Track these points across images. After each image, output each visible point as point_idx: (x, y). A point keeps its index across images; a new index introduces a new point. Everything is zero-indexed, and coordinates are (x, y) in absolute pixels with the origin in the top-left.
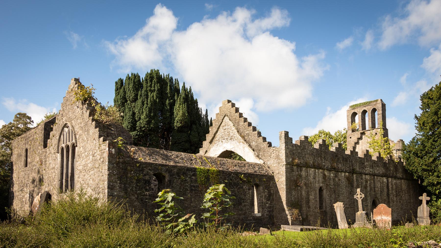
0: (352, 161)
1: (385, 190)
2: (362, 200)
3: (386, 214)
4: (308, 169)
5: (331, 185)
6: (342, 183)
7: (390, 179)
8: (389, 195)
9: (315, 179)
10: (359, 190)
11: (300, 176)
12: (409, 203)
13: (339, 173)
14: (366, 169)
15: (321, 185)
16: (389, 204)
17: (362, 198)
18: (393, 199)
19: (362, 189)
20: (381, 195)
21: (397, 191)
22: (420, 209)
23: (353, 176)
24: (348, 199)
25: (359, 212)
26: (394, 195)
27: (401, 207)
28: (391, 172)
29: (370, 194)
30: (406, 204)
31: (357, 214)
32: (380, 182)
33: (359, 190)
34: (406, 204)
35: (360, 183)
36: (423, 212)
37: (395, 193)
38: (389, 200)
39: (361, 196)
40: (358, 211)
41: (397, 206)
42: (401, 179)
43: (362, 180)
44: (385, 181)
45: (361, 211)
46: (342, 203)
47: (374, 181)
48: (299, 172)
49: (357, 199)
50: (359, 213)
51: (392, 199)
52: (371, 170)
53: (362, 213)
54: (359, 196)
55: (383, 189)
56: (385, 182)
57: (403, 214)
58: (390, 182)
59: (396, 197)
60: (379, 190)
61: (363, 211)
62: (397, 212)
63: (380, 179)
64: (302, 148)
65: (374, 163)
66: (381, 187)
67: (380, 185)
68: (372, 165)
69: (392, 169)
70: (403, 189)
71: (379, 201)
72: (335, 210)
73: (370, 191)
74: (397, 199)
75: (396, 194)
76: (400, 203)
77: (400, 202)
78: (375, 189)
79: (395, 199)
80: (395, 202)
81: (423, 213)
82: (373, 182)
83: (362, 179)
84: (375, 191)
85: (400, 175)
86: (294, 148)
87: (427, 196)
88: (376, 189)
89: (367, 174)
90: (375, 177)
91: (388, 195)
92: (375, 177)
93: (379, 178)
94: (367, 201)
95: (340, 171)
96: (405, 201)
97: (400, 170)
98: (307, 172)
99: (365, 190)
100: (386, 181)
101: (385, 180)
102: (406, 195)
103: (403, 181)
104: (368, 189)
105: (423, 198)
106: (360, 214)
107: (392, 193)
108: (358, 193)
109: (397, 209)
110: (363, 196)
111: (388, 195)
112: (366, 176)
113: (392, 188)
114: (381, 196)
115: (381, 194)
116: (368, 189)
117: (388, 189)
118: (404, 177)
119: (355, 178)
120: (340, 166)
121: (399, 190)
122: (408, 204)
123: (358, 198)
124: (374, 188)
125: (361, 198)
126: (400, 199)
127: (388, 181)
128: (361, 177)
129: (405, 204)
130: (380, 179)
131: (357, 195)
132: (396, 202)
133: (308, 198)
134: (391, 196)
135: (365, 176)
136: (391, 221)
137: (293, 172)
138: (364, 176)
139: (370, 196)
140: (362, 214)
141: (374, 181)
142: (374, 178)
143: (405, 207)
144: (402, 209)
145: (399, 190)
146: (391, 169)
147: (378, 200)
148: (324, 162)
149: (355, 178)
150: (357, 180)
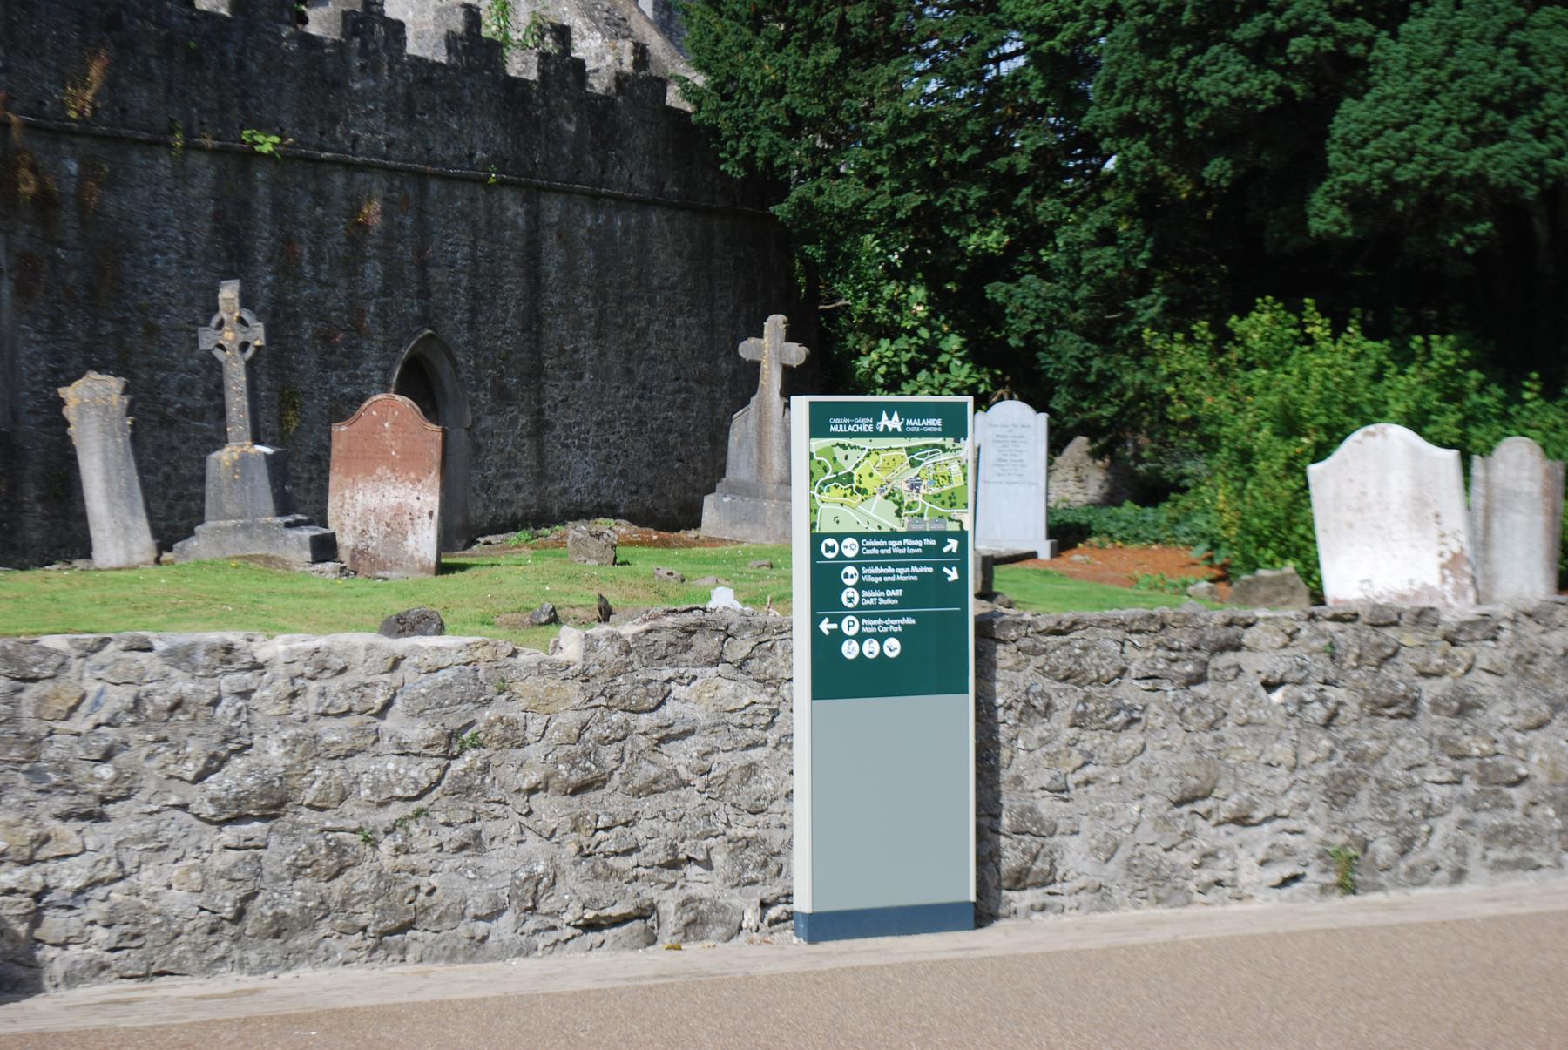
0: (241, 66)
1: (513, 285)
2: (250, 365)
3: (406, 466)
5: (61, 244)
6: (152, 226)
7: (553, 209)
8: (540, 319)
10: (229, 293)
12: (698, 381)
13: (136, 157)
16: (540, 389)
17: (250, 353)
18: (575, 351)
19: (323, 277)
22: (742, 426)
25: (227, 449)
26: (578, 325)
27: (638, 407)
28: (565, 150)
29: (383, 312)
30: (679, 391)
31: (218, 462)
32: (474, 224)
33: (229, 293)
34: (679, 391)
35: (304, 233)
36: (761, 451)
37: (587, 309)
38: (541, 360)
39: (241, 338)
40: (220, 441)
41: (600, 404)
42: (643, 204)
43: (319, 211)
44: (509, 214)
45: (239, 438)
46: (115, 384)
47: (421, 214)
49: (218, 353)
50: (224, 458)
51: (562, 351)
52: (401, 134)
53: (244, 458)
54: (228, 336)
56: (514, 226)
57: (649, 465)
58: (550, 226)
59: (599, 336)
60: (457, 283)
61: (257, 440)
62: (597, 447)
63: (473, 200)
65: (428, 81)
66: (475, 262)
67: (473, 246)
68: (408, 96)
69: (572, 128)
70: (655, 282)
71: (455, 364)
72: (72, 430)
73: (386, 291)
74: (602, 354)
75: (602, 313)
76: (631, 382)
77: (629, 371)
78: (424, 278)
79: (587, 348)
80: (588, 376)
81: (761, 464)
82: (408, 222)
83: (320, 198)
84: (425, 293)
85: (633, 174)
87: (790, 338)
88: (437, 275)
89: (365, 167)
90: (434, 186)
91: (533, 321)
92: (434, 186)
93: (461, 196)
94: (356, 367)
95: (137, 142)
96: (670, 370)
97: (640, 140)
99: (343, 282)
100: (521, 221)
101: (514, 208)
102: (678, 321)
103: (655, 217)
104: (373, 273)
105: (760, 349)
106: (235, 464)
108: (223, 314)
109: (599, 424)
110: (258, 335)
111: (533, 321)
112: (361, 177)
113: (568, 268)
114: (472, 326)
115: (473, 311)
117: (538, 279)
118: (671, 188)
119: (262, 190)
121: (622, 286)
122: (688, 390)
123: (221, 347)
124: (422, 265)
125: (244, 346)
126: (630, 353)
127: (534, 216)
128: (312, 186)
129: (671, 386)
130: (473, 200)
131: (221, 324)
132: (596, 373)
134: (558, 329)
135: (350, 182)
136: (436, 514)
138: (339, 180)
139: (386, 326)
140: (244, 461)
141: (421, 214)
142: (423, 192)
143: (670, 407)
144: (641, 422)
145: (622, 286)
146: (558, 127)
147: (451, 357)
149: (262, 190)
150: (278, 205)
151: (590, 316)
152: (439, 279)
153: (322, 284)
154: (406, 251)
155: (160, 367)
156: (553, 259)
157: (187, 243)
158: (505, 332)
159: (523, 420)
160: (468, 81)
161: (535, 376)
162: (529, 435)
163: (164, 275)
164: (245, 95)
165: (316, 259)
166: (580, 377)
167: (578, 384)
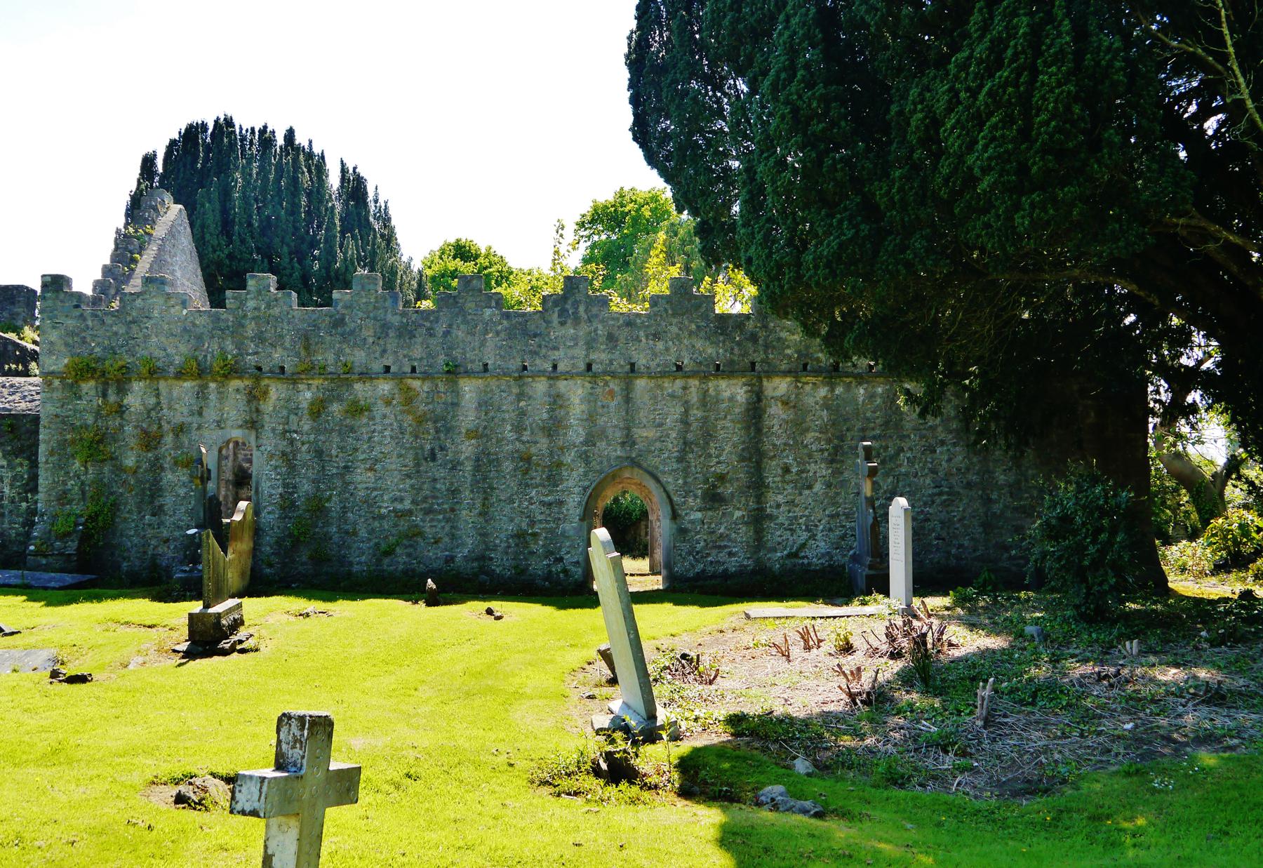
4: (162, 385)
7: (779, 386)
9: (200, 414)
11: (121, 410)
13: (358, 386)
14: (555, 355)
15: (237, 434)
19: (524, 438)
20: (680, 460)
21: (842, 438)
23: (457, 393)
24: (407, 481)
48: (112, 398)
55: (708, 435)
56: (731, 399)
60: (668, 436)
64: (129, 319)
73: (590, 441)
80: (818, 487)
84: (628, 441)
86: (90, 323)
88: (644, 434)
89: (569, 376)
91: (754, 455)
98: (158, 396)
101: (735, 391)
104: (576, 433)
107: (797, 445)
109: (832, 516)
116: (576, 433)
117: (759, 431)
120: (359, 357)
132: (829, 485)
133: (156, 482)
137: (80, 398)
148: (256, 353)
151: (822, 450)
152: (645, 435)
153: (524, 443)
154: (611, 420)
155: (375, 489)
156: (776, 414)
157: (400, 427)
158: (718, 463)
159: (738, 514)
160: (675, 321)
161: (757, 486)
162: (746, 523)
163: (380, 443)
164: (450, 348)
165: (519, 429)
166: (810, 487)
167: (807, 492)
